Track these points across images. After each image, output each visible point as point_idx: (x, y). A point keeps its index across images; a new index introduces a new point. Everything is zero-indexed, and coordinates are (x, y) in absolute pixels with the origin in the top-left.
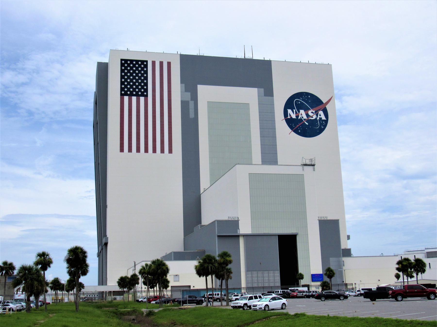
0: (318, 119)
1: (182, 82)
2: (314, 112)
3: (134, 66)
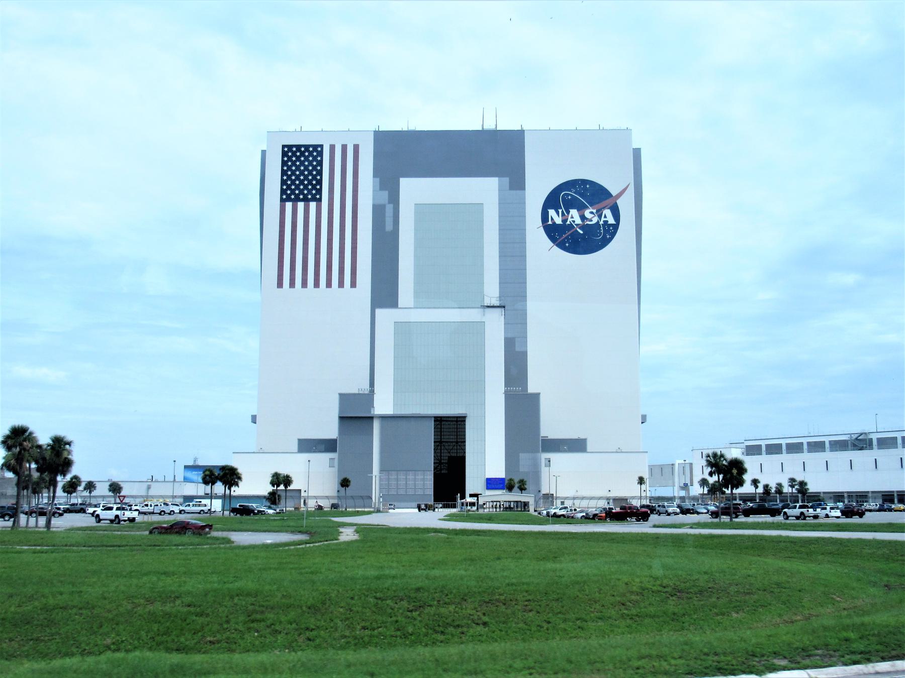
0: (601, 223)
1: (375, 175)
2: (594, 211)
3: (302, 154)
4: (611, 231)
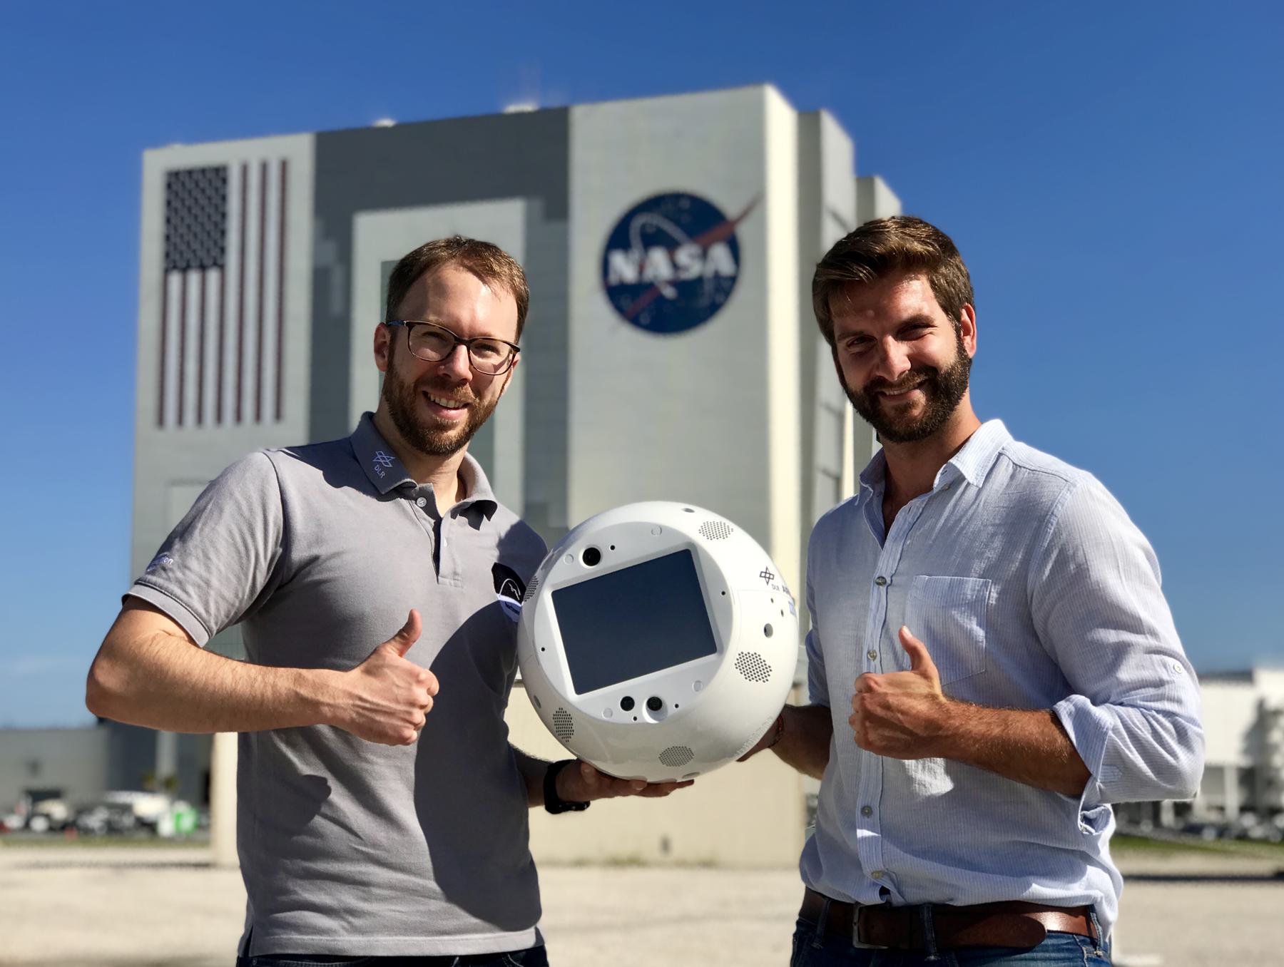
4: (724, 287)
